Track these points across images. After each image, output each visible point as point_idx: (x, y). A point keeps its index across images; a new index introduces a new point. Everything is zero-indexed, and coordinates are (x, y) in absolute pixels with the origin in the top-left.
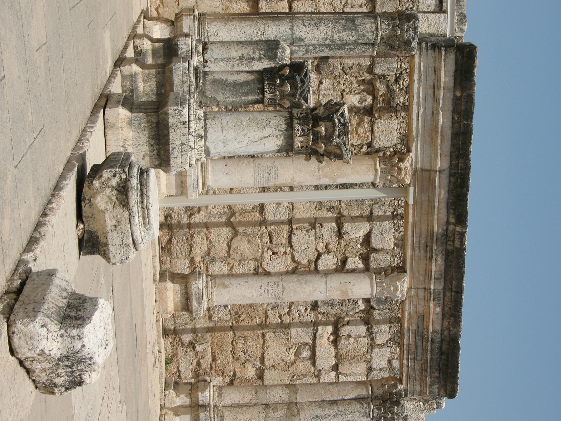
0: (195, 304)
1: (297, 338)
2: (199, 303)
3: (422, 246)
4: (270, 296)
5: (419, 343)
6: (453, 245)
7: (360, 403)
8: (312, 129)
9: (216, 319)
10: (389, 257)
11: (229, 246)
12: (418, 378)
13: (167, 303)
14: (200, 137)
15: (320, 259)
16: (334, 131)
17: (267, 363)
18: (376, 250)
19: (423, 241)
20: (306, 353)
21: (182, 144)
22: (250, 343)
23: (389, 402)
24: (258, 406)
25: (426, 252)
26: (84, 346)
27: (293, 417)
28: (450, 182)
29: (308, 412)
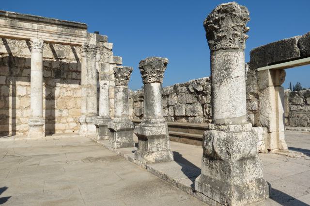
0: (38, 123)
3: (17, 31)
5: (63, 36)
12: (79, 38)
19: (14, 30)
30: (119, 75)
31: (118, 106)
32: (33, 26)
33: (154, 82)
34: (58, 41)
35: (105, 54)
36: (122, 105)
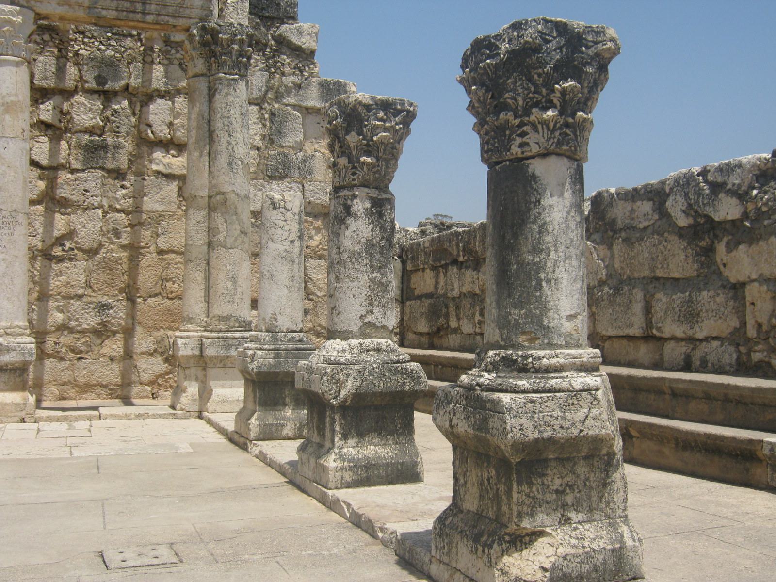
1: (170, 203)
4: (7, 231)
7: (214, 95)
10: (41, 58)
13: (6, 404)
15: (37, 162)
22: (172, 272)
23: (213, 47)
24: (211, 260)
27: (228, 203)
29: (221, 178)
30: (352, 138)
31: (345, 284)
33: (544, 155)
35: (287, 69)
36: (364, 280)
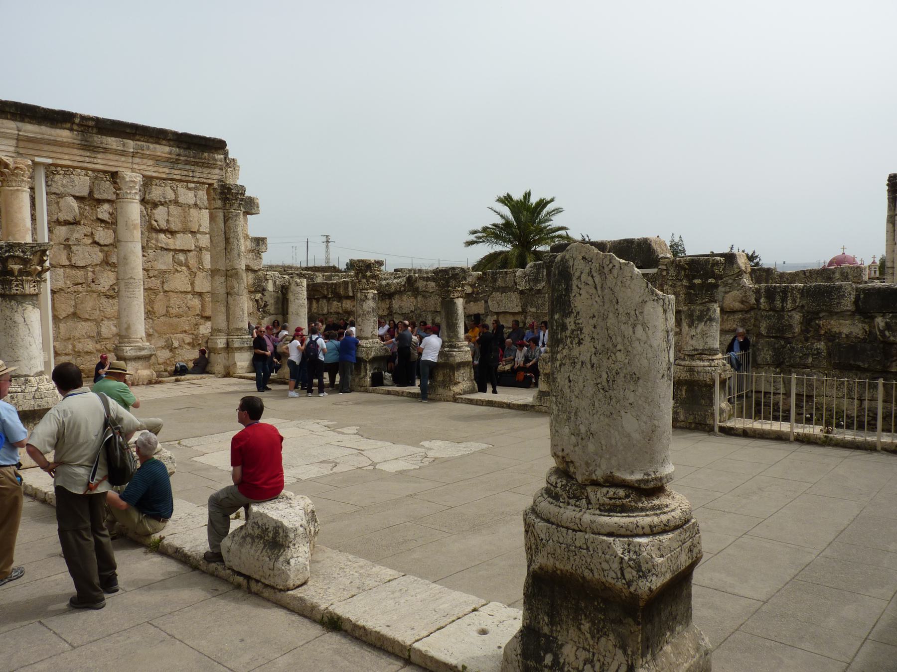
0: (143, 353)
2: (144, 349)
5: (180, 166)
6: (92, 127)
7: (228, 220)
8: (16, 277)
9: (151, 330)
11: (87, 320)
14: (27, 381)
16: (18, 257)
17: (189, 289)
18: (91, 193)
19: (88, 154)
20: (182, 257)
21: (34, 398)
25: (99, 152)
26: (301, 526)
28: (30, 123)
30: (368, 274)
32: (124, 145)
34: (170, 176)
36: (372, 320)
